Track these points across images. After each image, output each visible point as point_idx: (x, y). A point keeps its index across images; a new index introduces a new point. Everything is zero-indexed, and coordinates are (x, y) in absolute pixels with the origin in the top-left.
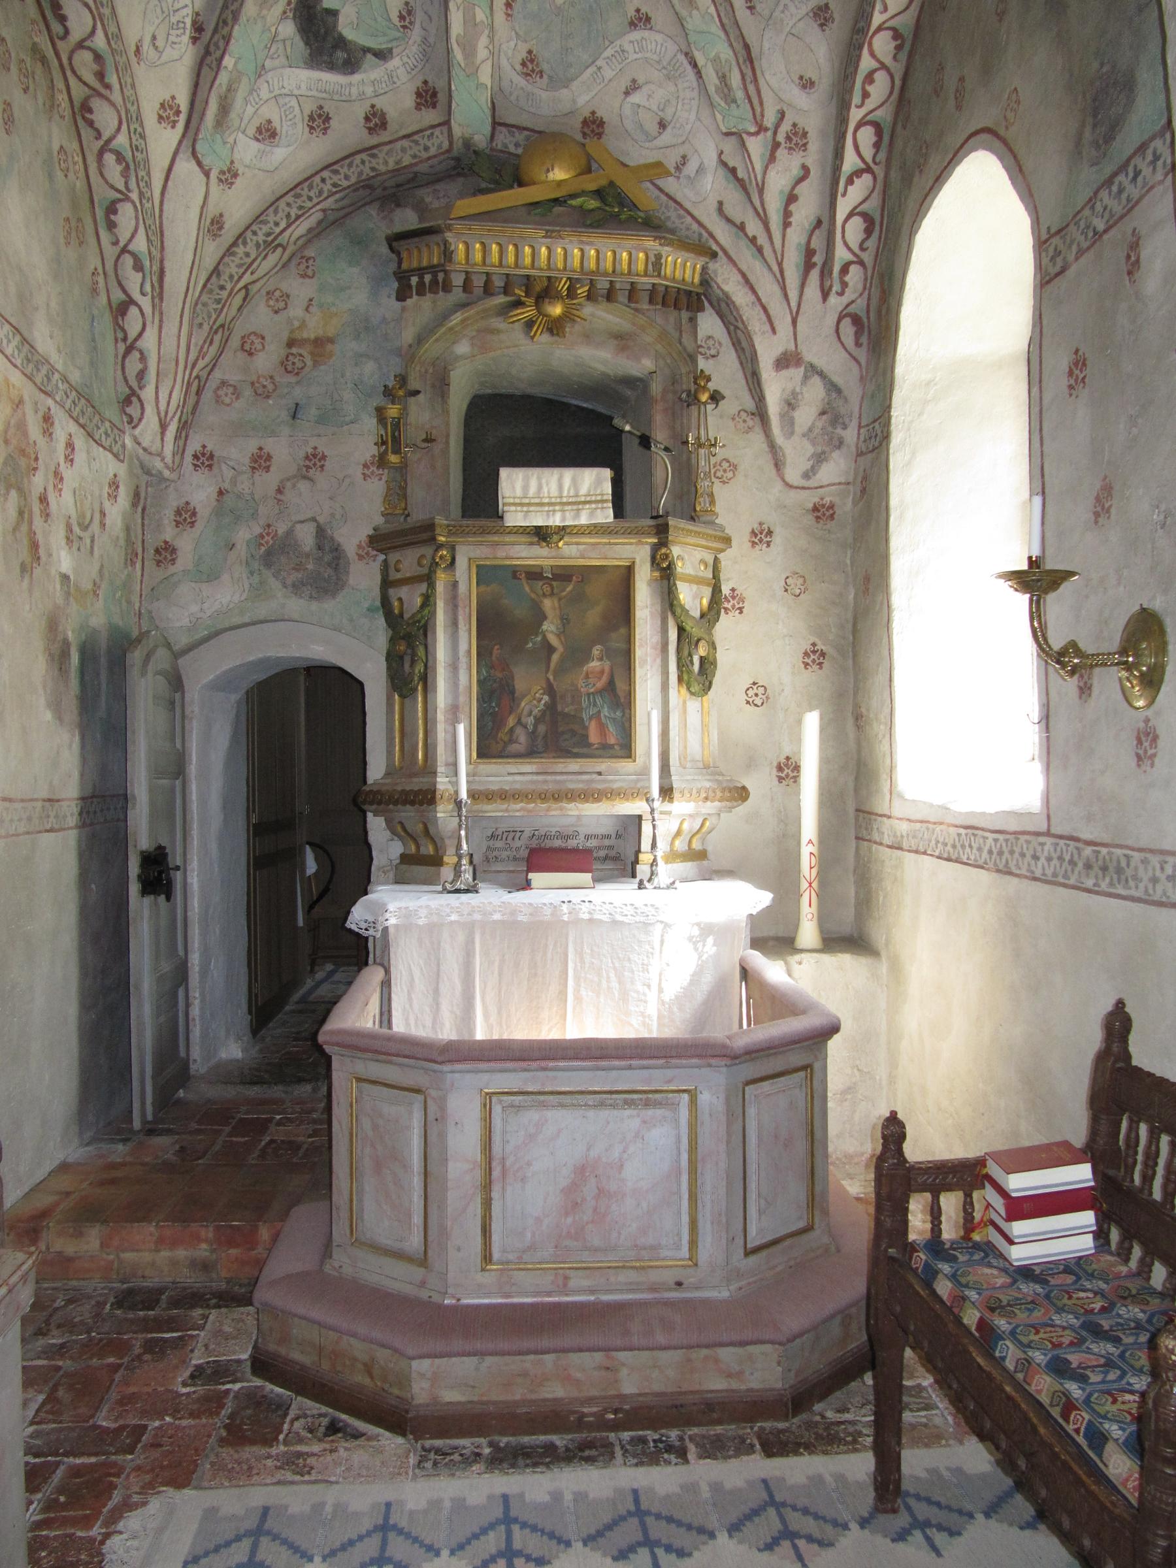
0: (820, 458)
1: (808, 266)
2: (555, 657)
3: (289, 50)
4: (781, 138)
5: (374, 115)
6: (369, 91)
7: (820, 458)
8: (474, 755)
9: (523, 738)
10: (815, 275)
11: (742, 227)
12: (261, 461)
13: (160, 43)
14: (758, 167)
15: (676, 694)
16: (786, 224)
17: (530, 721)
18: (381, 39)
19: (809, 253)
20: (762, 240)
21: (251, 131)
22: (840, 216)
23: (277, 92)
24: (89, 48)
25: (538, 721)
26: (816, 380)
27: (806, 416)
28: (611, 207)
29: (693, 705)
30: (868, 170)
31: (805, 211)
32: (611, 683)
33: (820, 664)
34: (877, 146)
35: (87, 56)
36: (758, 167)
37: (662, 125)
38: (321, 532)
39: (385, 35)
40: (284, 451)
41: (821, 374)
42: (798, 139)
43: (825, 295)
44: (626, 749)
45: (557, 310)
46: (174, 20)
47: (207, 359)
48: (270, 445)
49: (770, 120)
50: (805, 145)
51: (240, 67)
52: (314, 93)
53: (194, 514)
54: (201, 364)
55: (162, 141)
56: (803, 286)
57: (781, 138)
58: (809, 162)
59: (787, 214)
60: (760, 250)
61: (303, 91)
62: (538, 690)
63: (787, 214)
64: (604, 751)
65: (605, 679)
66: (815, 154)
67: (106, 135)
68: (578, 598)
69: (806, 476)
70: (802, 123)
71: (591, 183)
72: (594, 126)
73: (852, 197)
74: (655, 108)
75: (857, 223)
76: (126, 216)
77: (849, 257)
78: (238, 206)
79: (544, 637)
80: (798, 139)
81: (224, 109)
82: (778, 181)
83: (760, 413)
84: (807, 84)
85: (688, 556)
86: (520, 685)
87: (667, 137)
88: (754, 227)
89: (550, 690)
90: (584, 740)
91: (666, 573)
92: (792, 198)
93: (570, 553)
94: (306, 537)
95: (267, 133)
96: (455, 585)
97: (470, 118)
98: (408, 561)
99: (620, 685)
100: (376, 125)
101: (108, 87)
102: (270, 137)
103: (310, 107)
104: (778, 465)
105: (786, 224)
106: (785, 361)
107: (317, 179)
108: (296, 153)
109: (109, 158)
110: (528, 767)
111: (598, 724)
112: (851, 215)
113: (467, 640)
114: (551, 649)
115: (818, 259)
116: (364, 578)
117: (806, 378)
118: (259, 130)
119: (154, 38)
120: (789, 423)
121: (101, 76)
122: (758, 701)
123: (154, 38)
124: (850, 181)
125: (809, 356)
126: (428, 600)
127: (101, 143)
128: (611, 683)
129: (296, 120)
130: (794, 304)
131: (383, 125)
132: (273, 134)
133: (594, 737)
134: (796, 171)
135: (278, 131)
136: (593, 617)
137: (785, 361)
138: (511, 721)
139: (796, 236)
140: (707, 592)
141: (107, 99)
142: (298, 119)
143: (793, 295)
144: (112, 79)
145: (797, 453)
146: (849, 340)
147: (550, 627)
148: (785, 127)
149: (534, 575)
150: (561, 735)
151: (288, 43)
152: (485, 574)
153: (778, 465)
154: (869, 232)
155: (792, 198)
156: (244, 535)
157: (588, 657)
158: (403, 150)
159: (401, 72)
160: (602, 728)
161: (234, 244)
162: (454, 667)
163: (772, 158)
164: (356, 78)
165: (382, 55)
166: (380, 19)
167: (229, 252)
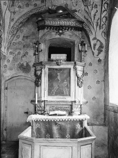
0: (99, 53)
1: (97, 25)
2: (59, 81)
4: (93, 6)
8: (47, 95)
9: (54, 93)
10: (98, 26)
11: (88, 20)
12: (19, 53)
14: (90, 11)
16: (94, 19)
17: (55, 91)
19: (98, 23)
20: (91, 21)
21: (17, 7)
22: (102, 17)
25: (57, 90)
26: (98, 42)
27: (97, 47)
30: (106, 10)
31: (98, 16)
32: (67, 85)
33: (99, 83)
34: (107, 7)
36: (90, 11)
37: (76, 5)
38: (27, 63)
40: (22, 52)
41: (99, 41)
42: (96, 6)
43: (100, 29)
44: (70, 95)
47: (12, 39)
48: (20, 51)
49: (91, 4)
50: (97, 7)
53: (9, 61)
54: (11, 40)
56: (97, 27)
57: (93, 6)
58: (97, 10)
59: (94, 17)
60: (90, 23)
62: (57, 86)
63: (94, 17)
65: (66, 85)
66: (99, 8)
69: (97, 56)
70: (97, 4)
73: (104, 14)
74: (75, 2)
75: (105, 18)
77: (103, 23)
79: (58, 79)
82: (93, 13)
83: (91, 46)
85: (79, 68)
86: (54, 85)
87: (77, 7)
88: (89, 19)
89: (58, 86)
91: (75, 69)
92: (95, 15)
93: (62, 66)
94: (25, 64)
96: (45, 71)
98: (38, 68)
99: (69, 85)
104: (93, 54)
105: (94, 19)
106: (95, 39)
110: (56, 97)
111: (65, 91)
112: (104, 17)
113: (47, 79)
114: (59, 80)
115: (99, 24)
116: (33, 69)
117: (97, 41)
120: (94, 48)
122: (90, 88)
124: (103, 12)
125: (98, 38)
126: (41, 73)
128: (67, 85)
130: (95, 31)
133: (65, 93)
134: (96, 11)
136: (65, 76)
137: (95, 39)
138: (53, 90)
139: (95, 21)
140: (82, 72)
143: (95, 29)
145: (96, 52)
146: (104, 36)
147: (59, 77)
148: (94, 4)
149: (56, 69)
150: (60, 93)
152: (49, 69)
153: (93, 54)
154: (106, 20)
155: (95, 15)
156: (16, 64)
157: (64, 82)
158: (39, 9)
160: (66, 92)
161: (15, 23)
162: (45, 83)
163: (92, 9)
167: (15, 24)
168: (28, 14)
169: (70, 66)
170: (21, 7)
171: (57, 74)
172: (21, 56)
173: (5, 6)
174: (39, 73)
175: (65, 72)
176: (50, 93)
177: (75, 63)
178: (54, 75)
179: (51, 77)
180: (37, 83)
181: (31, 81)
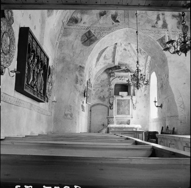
0: (145, 91)
7: (145, 91)
12: (99, 90)
15: (133, 110)
28: (128, 71)
29: (134, 111)
44: (129, 115)
45: (123, 78)
55: (94, 66)
64: (127, 115)
68: (125, 102)
69: (144, 92)
71: (126, 68)
72: (126, 64)
76: (91, 72)
78: (98, 70)
80: (143, 66)
84: (143, 62)
90: (125, 113)
93: (124, 98)
94: (102, 97)
95: (101, 65)
97: (116, 64)
99: (128, 109)
104: (141, 91)
108: (103, 66)
113: (116, 105)
116: (107, 100)
136: (126, 103)
149: (122, 100)
152: (118, 100)
153: (141, 91)
165: (109, 59)
169: (129, 98)
171: (122, 102)
172: (99, 92)
174: (111, 102)
175: (126, 101)
176: (118, 113)
177: (132, 97)
178: (120, 103)
179: (119, 104)
180: (111, 107)
181: (106, 106)
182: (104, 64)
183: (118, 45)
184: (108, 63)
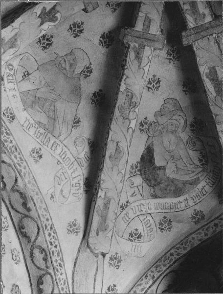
3: (141, 191)
5: (196, 214)
6: (191, 203)
13: (66, 192)
18: (192, 175)
21: (126, 236)
23: (138, 213)
24: (17, 191)
35: (17, 195)
39: (193, 172)
46: (74, 182)
51: (109, 195)
52: (159, 210)
61: (153, 210)
67: (33, 239)
81: (104, 218)
100: (199, 219)
101: (29, 210)
102: (138, 238)
103: (158, 219)
107: (168, 254)
109: (36, 252)
118: (131, 235)
119: (62, 191)
121: (25, 204)
123: (62, 191)
127: (31, 244)
129: (152, 227)
131: (203, 217)
132: (140, 237)
135: (142, 234)
141: (31, 218)
142: (153, 226)
144: (30, 205)
151: (140, 188)
159: (207, 188)
164: (181, 198)
165: (195, 182)
166: (188, 165)
168: (172, 254)
170: (140, 237)
173: (73, 236)
182: (166, 224)
183: (191, 23)
184: (190, 212)
